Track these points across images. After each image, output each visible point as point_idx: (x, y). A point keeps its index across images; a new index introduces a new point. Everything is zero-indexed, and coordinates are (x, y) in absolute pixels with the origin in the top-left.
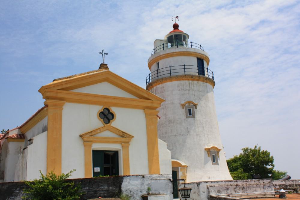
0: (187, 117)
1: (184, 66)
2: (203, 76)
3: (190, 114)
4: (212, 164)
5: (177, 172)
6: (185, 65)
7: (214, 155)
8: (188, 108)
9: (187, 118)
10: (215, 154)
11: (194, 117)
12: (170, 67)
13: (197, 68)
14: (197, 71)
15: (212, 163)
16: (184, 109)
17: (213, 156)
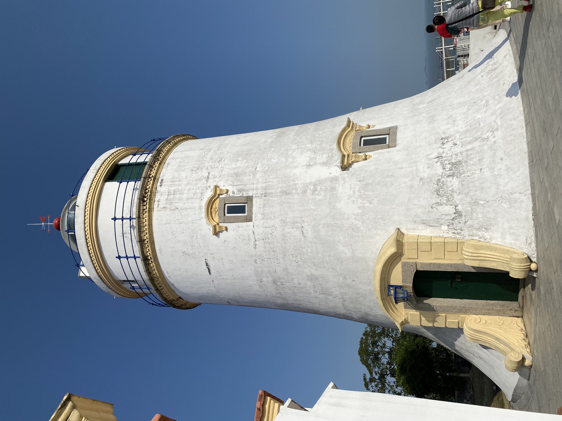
0: (249, 219)
1: (115, 219)
2: (147, 167)
3: (241, 210)
4: (395, 146)
5: (420, 269)
6: (113, 217)
7: (364, 140)
8: (227, 215)
9: (250, 220)
10: (362, 137)
11: (249, 199)
12: (119, 257)
13: (124, 184)
14: (132, 184)
15: (389, 147)
16: (226, 229)
17: (367, 143)
